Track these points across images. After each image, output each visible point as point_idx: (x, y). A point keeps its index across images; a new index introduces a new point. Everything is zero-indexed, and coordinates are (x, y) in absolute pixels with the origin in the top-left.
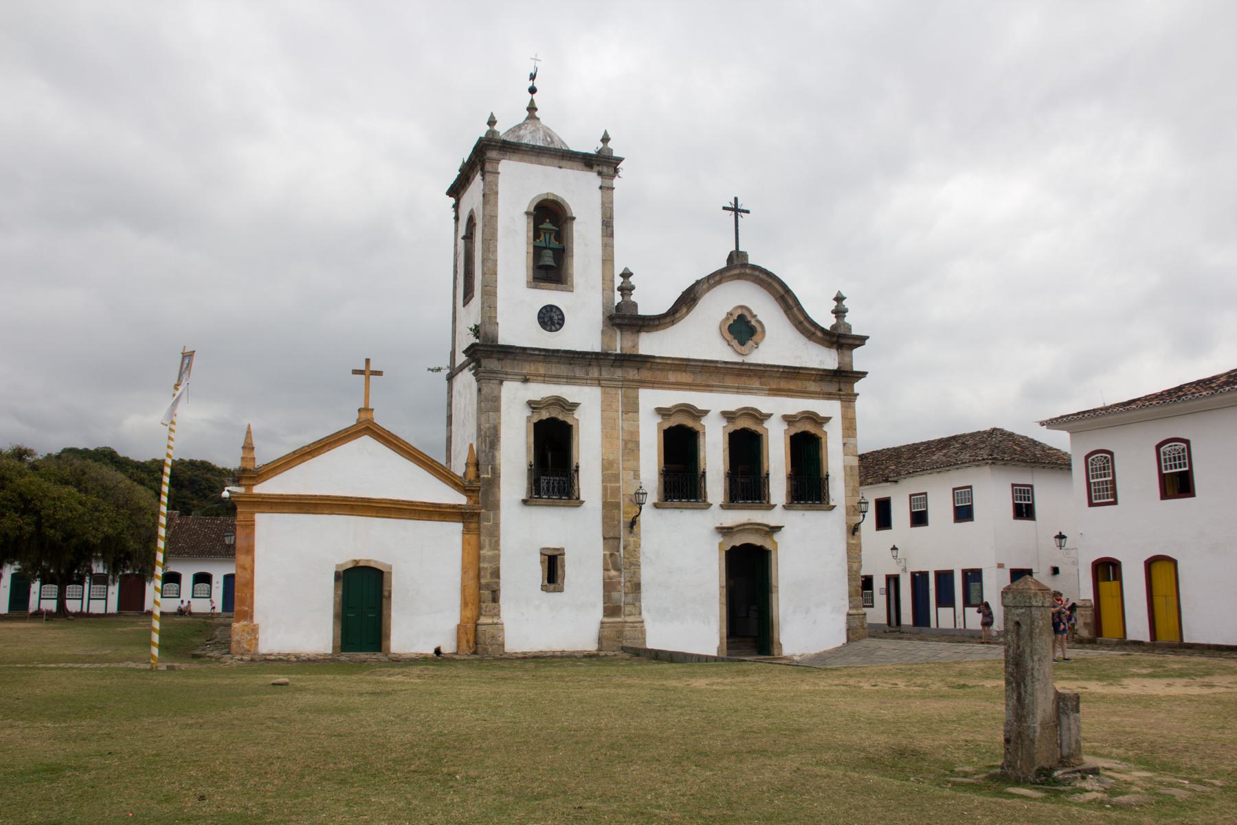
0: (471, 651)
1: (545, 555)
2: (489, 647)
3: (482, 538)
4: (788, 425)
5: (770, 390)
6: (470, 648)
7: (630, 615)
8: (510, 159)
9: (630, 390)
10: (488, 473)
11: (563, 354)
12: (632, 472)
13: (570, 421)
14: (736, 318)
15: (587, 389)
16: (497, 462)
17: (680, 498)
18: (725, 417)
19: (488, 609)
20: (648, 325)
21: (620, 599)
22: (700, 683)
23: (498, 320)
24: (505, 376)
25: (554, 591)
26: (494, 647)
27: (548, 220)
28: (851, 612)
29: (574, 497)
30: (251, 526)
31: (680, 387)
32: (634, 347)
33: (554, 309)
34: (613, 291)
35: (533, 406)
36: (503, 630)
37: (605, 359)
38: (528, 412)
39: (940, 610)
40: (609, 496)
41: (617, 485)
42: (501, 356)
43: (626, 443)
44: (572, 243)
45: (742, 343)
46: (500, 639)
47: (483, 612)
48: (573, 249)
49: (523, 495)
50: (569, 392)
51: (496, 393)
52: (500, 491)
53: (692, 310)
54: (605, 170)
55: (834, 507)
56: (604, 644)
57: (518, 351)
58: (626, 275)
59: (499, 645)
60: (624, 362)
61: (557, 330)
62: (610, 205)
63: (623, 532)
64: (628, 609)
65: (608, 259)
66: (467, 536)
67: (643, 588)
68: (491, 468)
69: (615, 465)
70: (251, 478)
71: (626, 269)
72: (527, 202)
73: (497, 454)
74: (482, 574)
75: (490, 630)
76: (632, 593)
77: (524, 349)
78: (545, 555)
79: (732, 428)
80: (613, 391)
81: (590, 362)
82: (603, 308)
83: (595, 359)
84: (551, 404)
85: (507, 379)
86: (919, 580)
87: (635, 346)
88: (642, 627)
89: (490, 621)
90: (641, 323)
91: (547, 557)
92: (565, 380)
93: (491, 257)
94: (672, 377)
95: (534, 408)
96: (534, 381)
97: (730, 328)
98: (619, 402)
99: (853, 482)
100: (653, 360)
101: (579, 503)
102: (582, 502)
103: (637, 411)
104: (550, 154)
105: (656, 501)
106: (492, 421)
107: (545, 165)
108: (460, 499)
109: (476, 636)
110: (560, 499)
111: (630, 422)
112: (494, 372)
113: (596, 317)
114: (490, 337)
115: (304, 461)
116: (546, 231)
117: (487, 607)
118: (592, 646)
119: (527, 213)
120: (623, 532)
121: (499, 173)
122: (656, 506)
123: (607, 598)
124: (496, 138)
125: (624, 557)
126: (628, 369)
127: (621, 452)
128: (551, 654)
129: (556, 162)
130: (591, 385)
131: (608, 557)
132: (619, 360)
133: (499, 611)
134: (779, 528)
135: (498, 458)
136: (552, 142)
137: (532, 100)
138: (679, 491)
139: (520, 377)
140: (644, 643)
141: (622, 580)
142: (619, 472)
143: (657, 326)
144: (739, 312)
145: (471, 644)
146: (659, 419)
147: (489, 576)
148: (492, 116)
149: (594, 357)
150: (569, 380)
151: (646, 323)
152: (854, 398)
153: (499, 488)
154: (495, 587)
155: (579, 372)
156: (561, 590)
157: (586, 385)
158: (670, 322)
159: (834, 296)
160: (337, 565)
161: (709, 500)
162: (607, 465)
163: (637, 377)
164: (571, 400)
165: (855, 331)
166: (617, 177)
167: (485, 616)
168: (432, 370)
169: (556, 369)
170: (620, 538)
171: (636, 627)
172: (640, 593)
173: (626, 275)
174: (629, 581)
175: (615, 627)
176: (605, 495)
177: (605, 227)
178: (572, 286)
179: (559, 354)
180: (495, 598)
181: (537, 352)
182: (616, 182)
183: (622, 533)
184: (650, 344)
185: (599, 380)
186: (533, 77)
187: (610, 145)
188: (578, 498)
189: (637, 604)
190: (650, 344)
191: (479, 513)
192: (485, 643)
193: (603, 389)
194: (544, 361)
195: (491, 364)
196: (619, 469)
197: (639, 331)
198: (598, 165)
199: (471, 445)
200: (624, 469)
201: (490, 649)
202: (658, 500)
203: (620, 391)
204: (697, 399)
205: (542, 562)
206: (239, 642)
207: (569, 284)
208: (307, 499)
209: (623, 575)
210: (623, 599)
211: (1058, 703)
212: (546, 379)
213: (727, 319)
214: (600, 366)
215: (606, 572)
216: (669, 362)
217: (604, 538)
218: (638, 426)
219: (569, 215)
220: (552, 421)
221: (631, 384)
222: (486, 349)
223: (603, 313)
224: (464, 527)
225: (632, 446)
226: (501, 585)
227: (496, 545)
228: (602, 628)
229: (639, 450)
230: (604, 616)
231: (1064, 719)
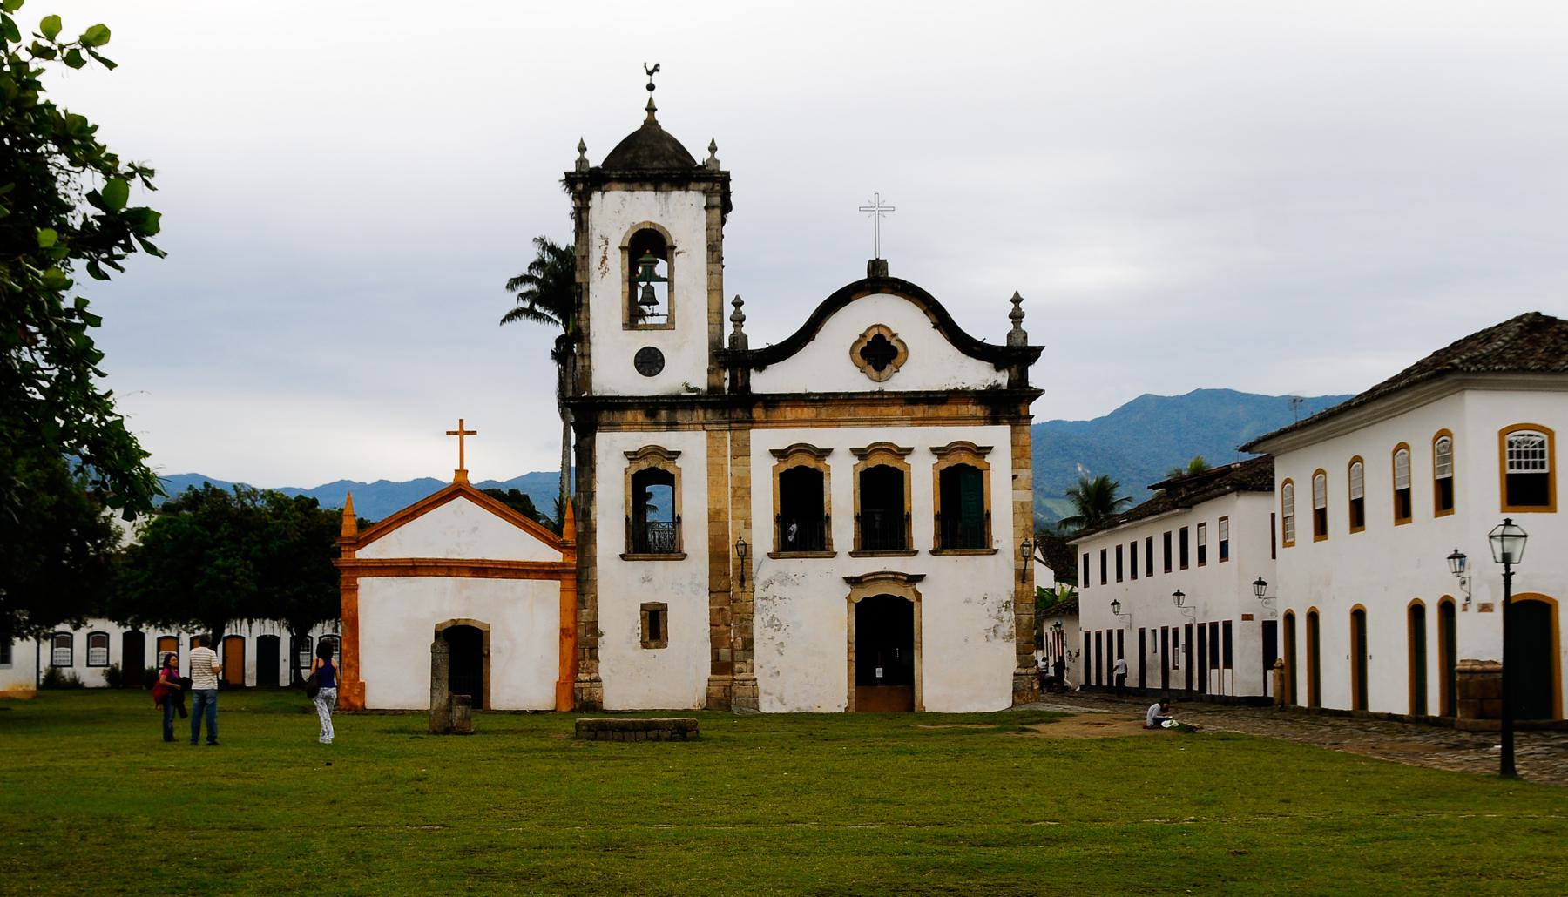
4: (939, 459)
5: (912, 419)
9: (737, 433)
13: (671, 470)
14: (870, 340)
18: (855, 455)
28: (1017, 672)
31: (799, 424)
34: (722, 324)
38: (626, 463)
39: (1212, 670)
43: (735, 490)
45: (879, 367)
49: (622, 551)
55: (996, 551)
65: (715, 288)
69: (722, 514)
73: (592, 509)
79: (862, 466)
84: (649, 454)
89: (587, 678)
97: (865, 353)
98: (726, 446)
99: (1025, 520)
105: (771, 551)
119: (622, 248)
134: (920, 578)
135: (593, 513)
137: (651, 99)
144: (875, 331)
148: (582, 142)
152: (1028, 420)
153: (595, 544)
159: (1012, 297)
160: (436, 625)
162: (715, 517)
165: (1032, 342)
173: (738, 303)
184: (761, 383)
185: (703, 424)
188: (680, 552)
189: (749, 661)
190: (761, 383)
200: (733, 518)
203: (729, 435)
204: (817, 437)
218: (749, 472)
219: (669, 243)
225: (742, 492)
229: (750, 497)
230: (712, 673)
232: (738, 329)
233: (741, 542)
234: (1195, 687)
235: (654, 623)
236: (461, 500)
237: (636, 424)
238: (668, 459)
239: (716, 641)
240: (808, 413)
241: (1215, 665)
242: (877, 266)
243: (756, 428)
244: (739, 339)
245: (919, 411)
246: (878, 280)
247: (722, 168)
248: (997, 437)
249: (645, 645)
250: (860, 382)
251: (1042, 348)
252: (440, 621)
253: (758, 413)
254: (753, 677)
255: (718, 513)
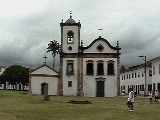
15: (75, 58)
30: (31, 78)
34: (80, 44)
38: (67, 62)
45: (100, 50)
50: (72, 59)
55: (115, 75)
58: (82, 41)
72: (67, 32)
79: (98, 63)
86: (139, 85)
97: (98, 48)
103: (83, 61)
108: (57, 74)
119: (67, 33)
123: (78, 89)
134: (105, 78)
161: (94, 74)
173: (82, 41)
184: (85, 52)
186: (71, 12)
190: (85, 52)
213: (97, 47)
225: (82, 66)
234: (137, 93)
235: (70, 84)
236: (45, 66)
239: (78, 86)
240: (91, 56)
241: (141, 90)
242: (100, 37)
245: (106, 56)
246: (100, 39)
248: (115, 60)
249: (69, 87)
250: (98, 52)
251: (121, 48)
252: (42, 83)
253: (84, 56)
255: (79, 69)
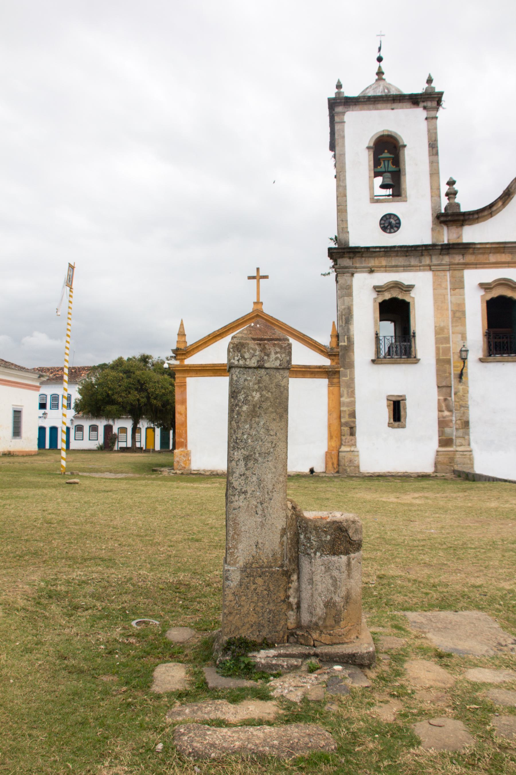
0: (336, 471)
1: (391, 400)
2: (347, 468)
3: (341, 389)
6: (335, 469)
7: (461, 446)
8: (353, 110)
9: (456, 272)
10: (345, 342)
11: (399, 249)
12: (460, 336)
13: (407, 299)
16: (351, 333)
17: (501, 353)
19: (347, 441)
20: (469, 219)
21: (452, 434)
22: (408, 498)
23: (349, 230)
24: (355, 270)
25: (398, 427)
26: (352, 468)
27: (386, 151)
29: (412, 357)
30: (184, 386)
31: (500, 265)
32: (458, 238)
33: (392, 217)
34: (440, 197)
35: (377, 290)
36: (358, 456)
37: (433, 249)
38: (374, 295)
40: (441, 355)
41: (448, 345)
42: (352, 255)
43: (454, 312)
44: (404, 164)
46: (356, 462)
47: (343, 443)
48: (405, 169)
51: (349, 283)
52: (354, 354)
53: (508, 203)
54: (429, 104)
56: (439, 467)
57: (363, 250)
58: (451, 183)
59: (355, 467)
60: (450, 250)
61: (395, 232)
62: (435, 131)
63: (454, 382)
64: (459, 441)
65: (434, 173)
66: (331, 388)
67: (471, 425)
68: (347, 338)
69: (446, 330)
70: (183, 354)
71: (451, 178)
73: (350, 327)
74: (342, 415)
75: (348, 456)
76: (462, 428)
77: (368, 248)
78: (391, 400)
80: (441, 274)
81: (422, 253)
82: (432, 211)
83: (425, 250)
85: (356, 272)
87: (460, 236)
88: (470, 455)
89: (348, 449)
90: (462, 218)
91: (392, 402)
92: (402, 268)
93: (342, 184)
94: (492, 258)
95: (378, 292)
96: (378, 271)
98: (447, 281)
100: (473, 246)
101: (416, 361)
102: (419, 360)
103: (463, 288)
104: (383, 100)
106: (346, 304)
107: (380, 109)
108: (326, 362)
109: (338, 460)
110: (401, 358)
111: (457, 297)
112: (346, 268)
113: (428, 218)
114: (343, 242)
115: (216, 341)
116: (385, 159)
117: (346, 439)
118: (429, 469)
120: (454, 382)
121: (344, 122)
122: (481, 360)
123: (441, 433)
124: (341, 96)
125: (455, 401)
126: (454, 256)
127: (450, 320)
128: (378, 474)
129: (389, 105)
130: (424, 270)
131: (441, 401)
132: (445, 249)
133: (355, 442)
136: (389, 92)
137: (380, 67)
138: (500, 348)
139: (367, 270)
140: (472, 467)
141: (454, 418)
142: (449, 336)
143: (478, 218)
145: (335, 466)
146: (482, 292)
147: (347, 416)
148: (339, 82)
149: (424, 248)
150: (405, 268)
151: (467, 217)
153: (353, 352)
154: (352, 425)
155: (413, 261)
156: (404, 427)
157: (420, 270)
158: (489, 214)
163: (462, 261)
164: (406, 283)
166: (440, 109)
167: (345, 445)
168: (324, 275)
169: (394, 261)
170: (451, 387)
171: (465, 455)
172: (469, 429)
173: (451, 183)
174: (460, 419)
175: (448, 455)
176: (437, 353)
177: (431, 149)
178: (406, 197)
179: (396, 249)
180: (352, 432)
181: (378, 250)
182: (441, 113)
183: (453, 383)
187: (433, 85)
188: (415, 357)
189: (467, 437)
191: (339, 371)
192: (344, 465)
193: (434, 272)
194: (385, 256)
195: (345, 262)
196: (448, 333)
197: (462, 225)
198: (423, 102)
199: (334, 322)
200: (453, 333)
201: (348, 470)
202: (484, 356)
203: (448, 274)
205: (388, 406)
206: (178, 462)
207: (403, 196)
208: (218, 366)
209: (454, 415)
210: (454, 433)
211: (297, 535)
212: (387, 269)
214: (431, 255)
215: (440, 413)
216: (488, 246)
217: (438, 387)
218: (464, 299)
219: (401, 144)
220: (394, 301)
221: (457, 266)
222: (338, 251)
223: (432, 214)
224: (329, 382)
226: (357, 423)
227: (352, 394)
228: (437, 455)
229: (465, 318)
231: (305, 562)
232: (451, 201)
233: (463, 349)
237: (382, 267)
238: (405, 291)
243: (468, 268)
244: (453, 206)
247: (437, 90)
254: (468, 449)
